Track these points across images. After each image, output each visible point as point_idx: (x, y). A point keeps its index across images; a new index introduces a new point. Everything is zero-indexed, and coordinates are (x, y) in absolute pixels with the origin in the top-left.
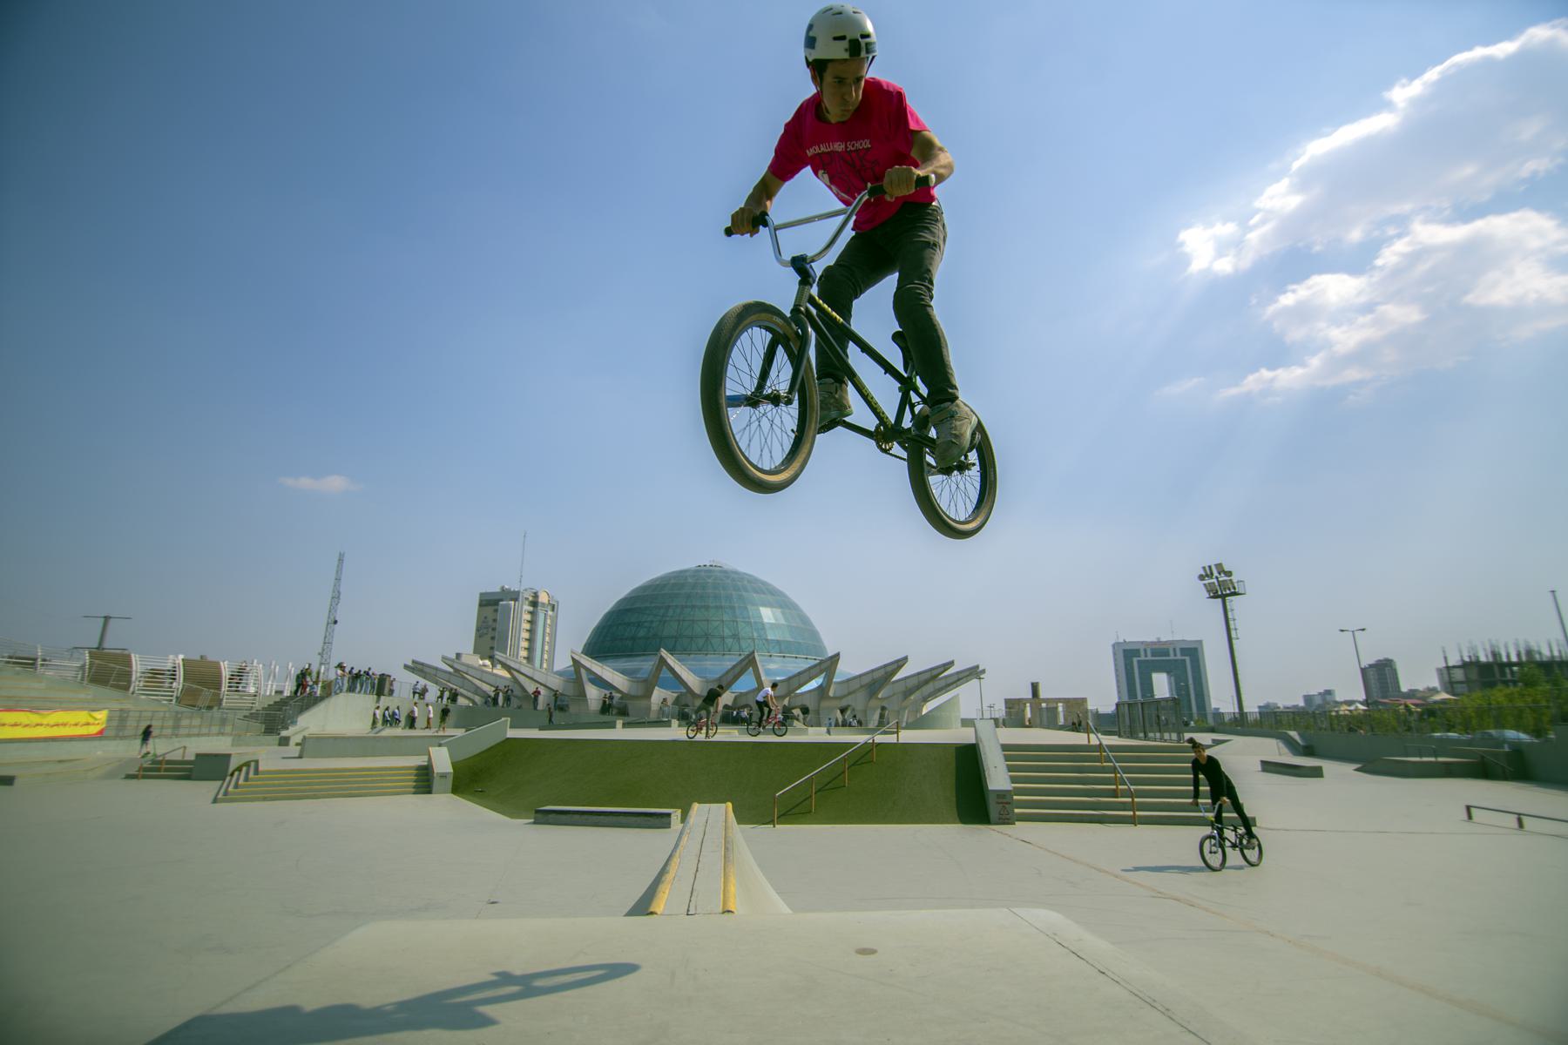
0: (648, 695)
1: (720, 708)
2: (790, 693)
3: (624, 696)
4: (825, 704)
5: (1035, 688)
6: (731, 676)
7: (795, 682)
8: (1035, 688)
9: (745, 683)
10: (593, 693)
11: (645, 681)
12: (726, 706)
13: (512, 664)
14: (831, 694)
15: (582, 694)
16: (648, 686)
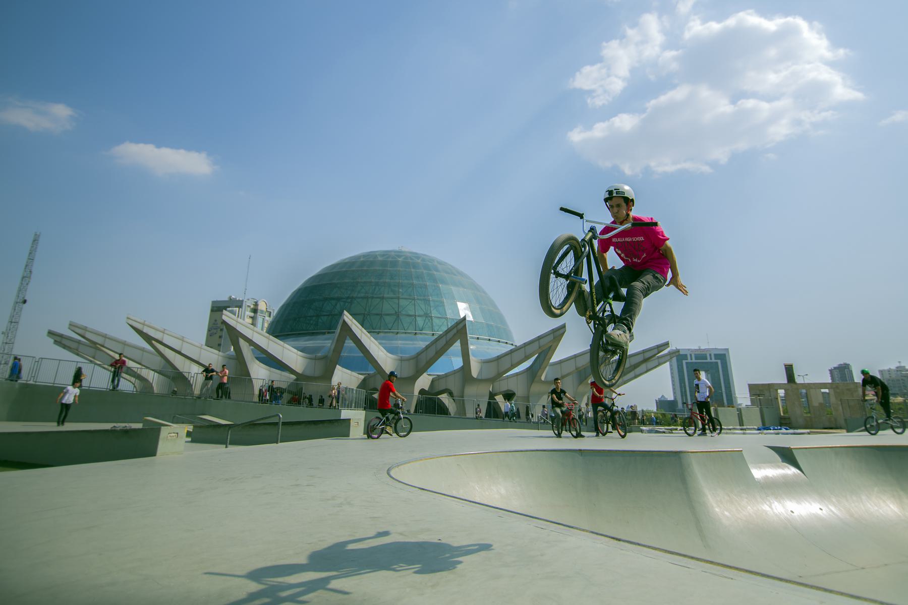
0: (328, 375)
1: (416, 393)
2: (500, 375)
3: (300, 377)
4: (535, 388)
5: (789, 370)
6: (431, 352)
7: (506, 362)
8: (789, 370)
9: (452, 361)
10: (260, 374)
11: (325, 358)
12: (422, 392)
13: (152, 333)
14: (543, 378)
15: (243, 374)
16: (328, 365)
